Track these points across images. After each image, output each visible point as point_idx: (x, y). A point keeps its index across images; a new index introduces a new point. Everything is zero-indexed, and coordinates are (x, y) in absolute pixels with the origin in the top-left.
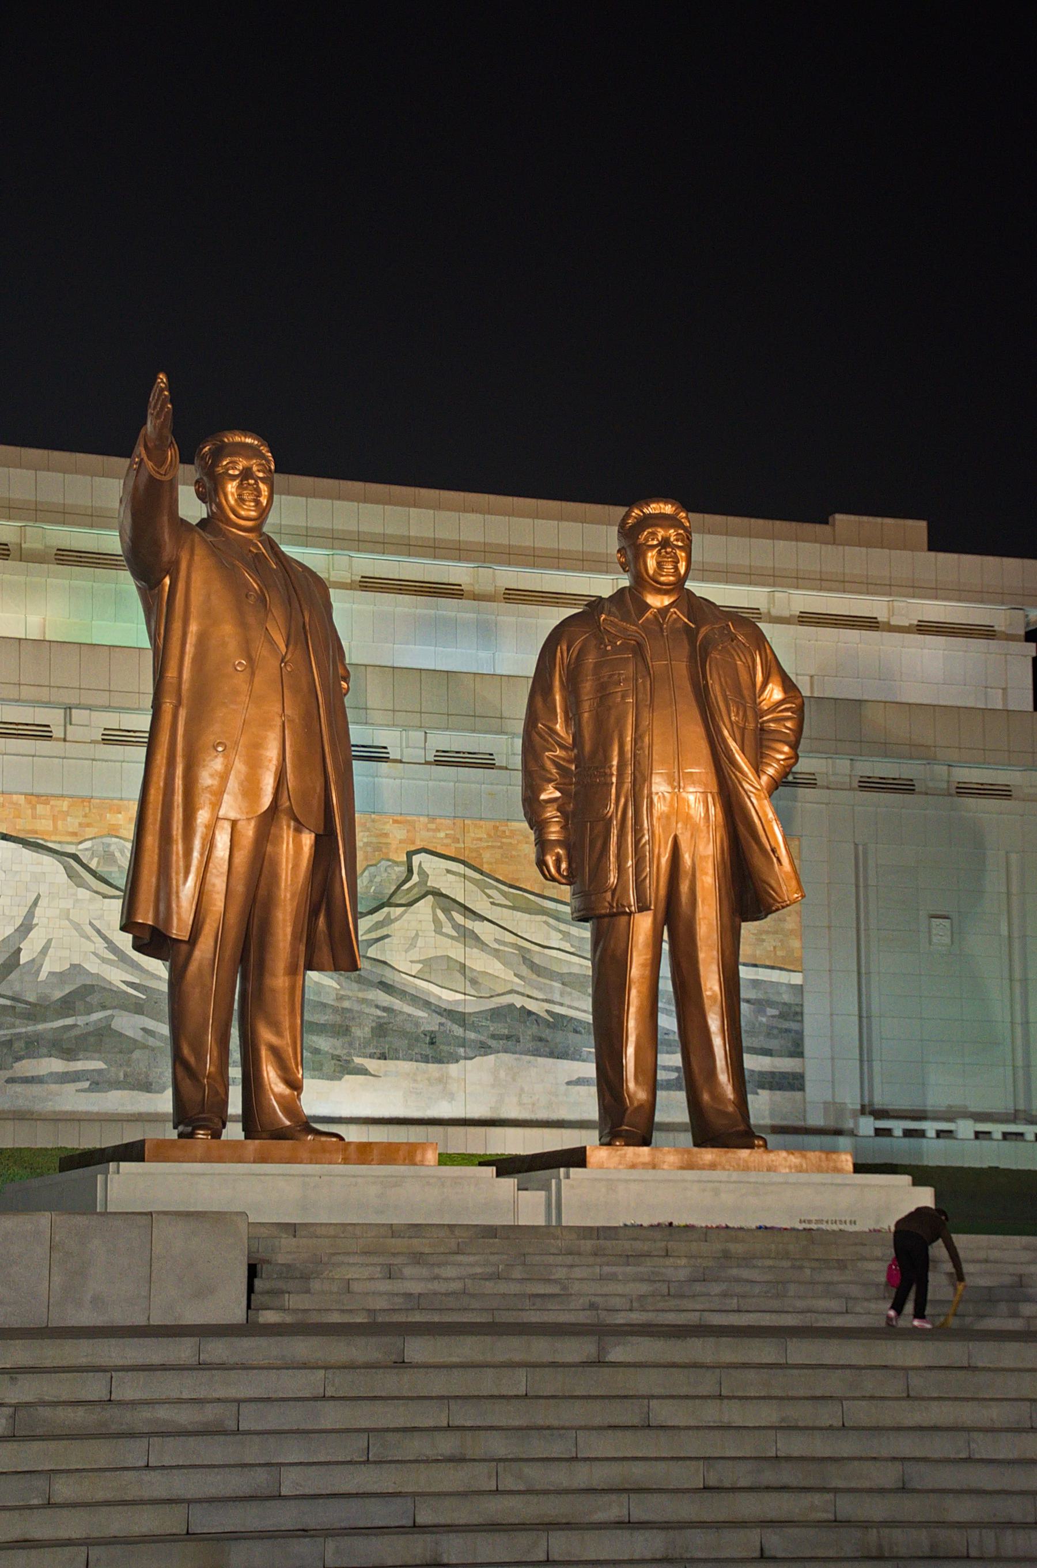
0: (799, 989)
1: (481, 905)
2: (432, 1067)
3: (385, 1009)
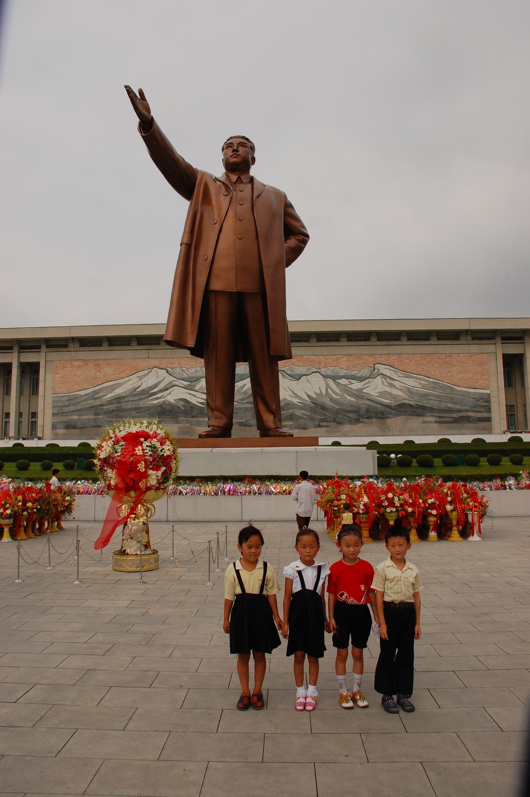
0: (489, 395)
1: (395, 377)
2: (383, 421)
3: (369, 406)
